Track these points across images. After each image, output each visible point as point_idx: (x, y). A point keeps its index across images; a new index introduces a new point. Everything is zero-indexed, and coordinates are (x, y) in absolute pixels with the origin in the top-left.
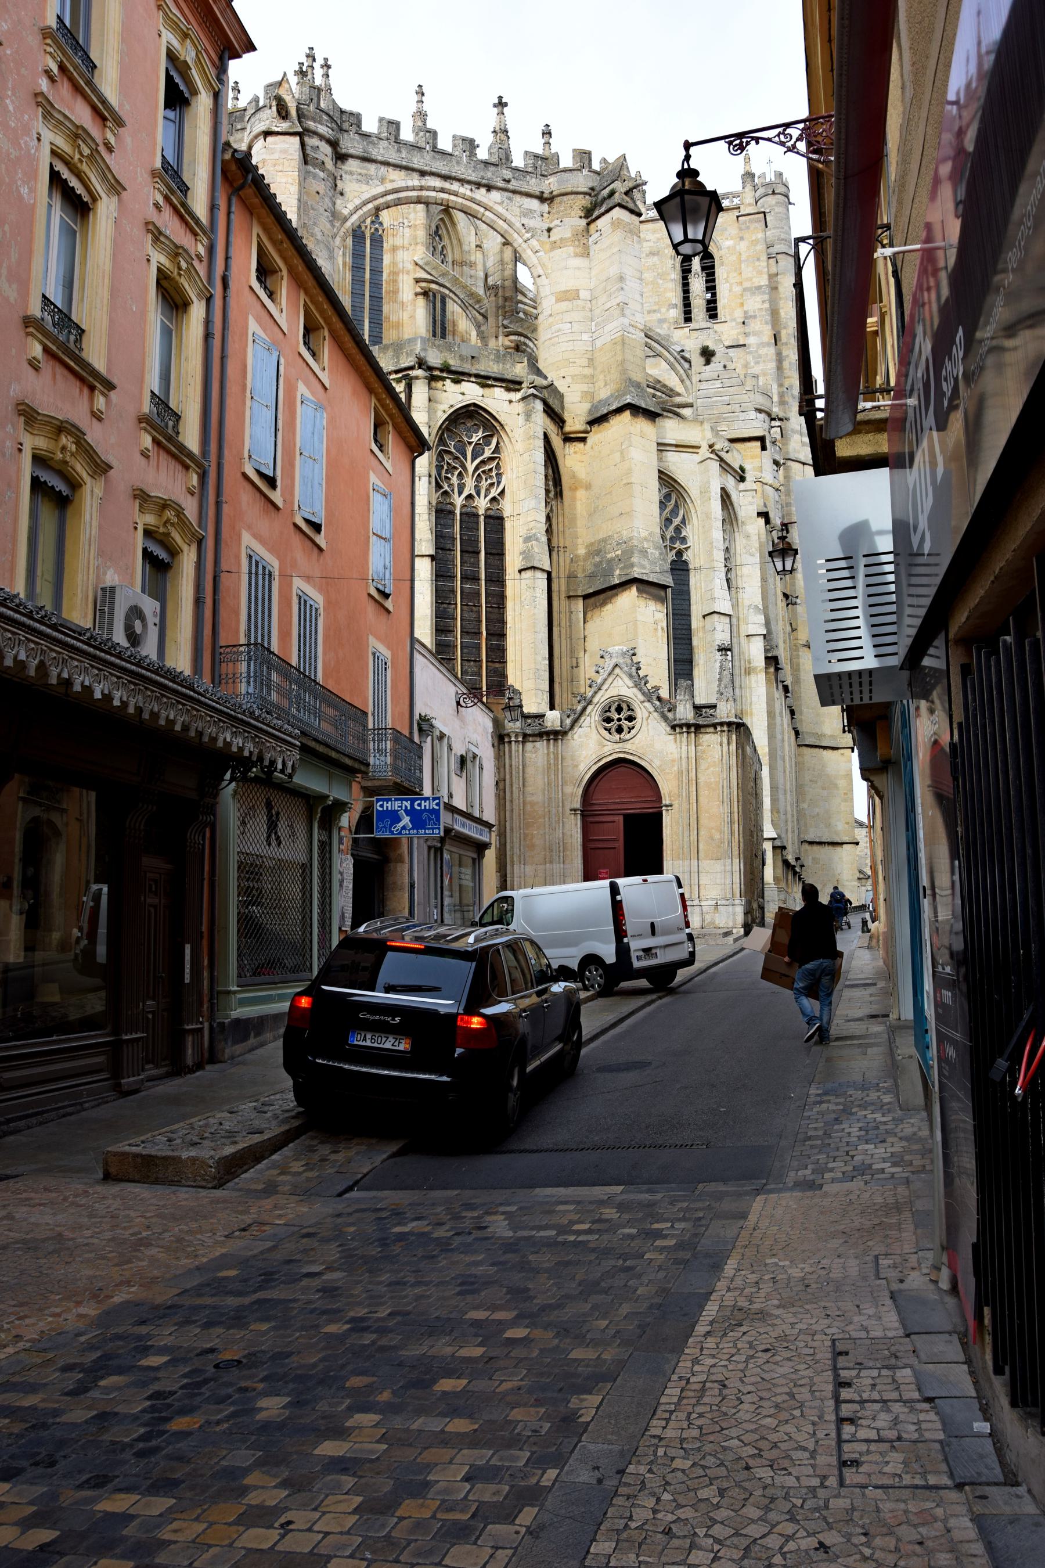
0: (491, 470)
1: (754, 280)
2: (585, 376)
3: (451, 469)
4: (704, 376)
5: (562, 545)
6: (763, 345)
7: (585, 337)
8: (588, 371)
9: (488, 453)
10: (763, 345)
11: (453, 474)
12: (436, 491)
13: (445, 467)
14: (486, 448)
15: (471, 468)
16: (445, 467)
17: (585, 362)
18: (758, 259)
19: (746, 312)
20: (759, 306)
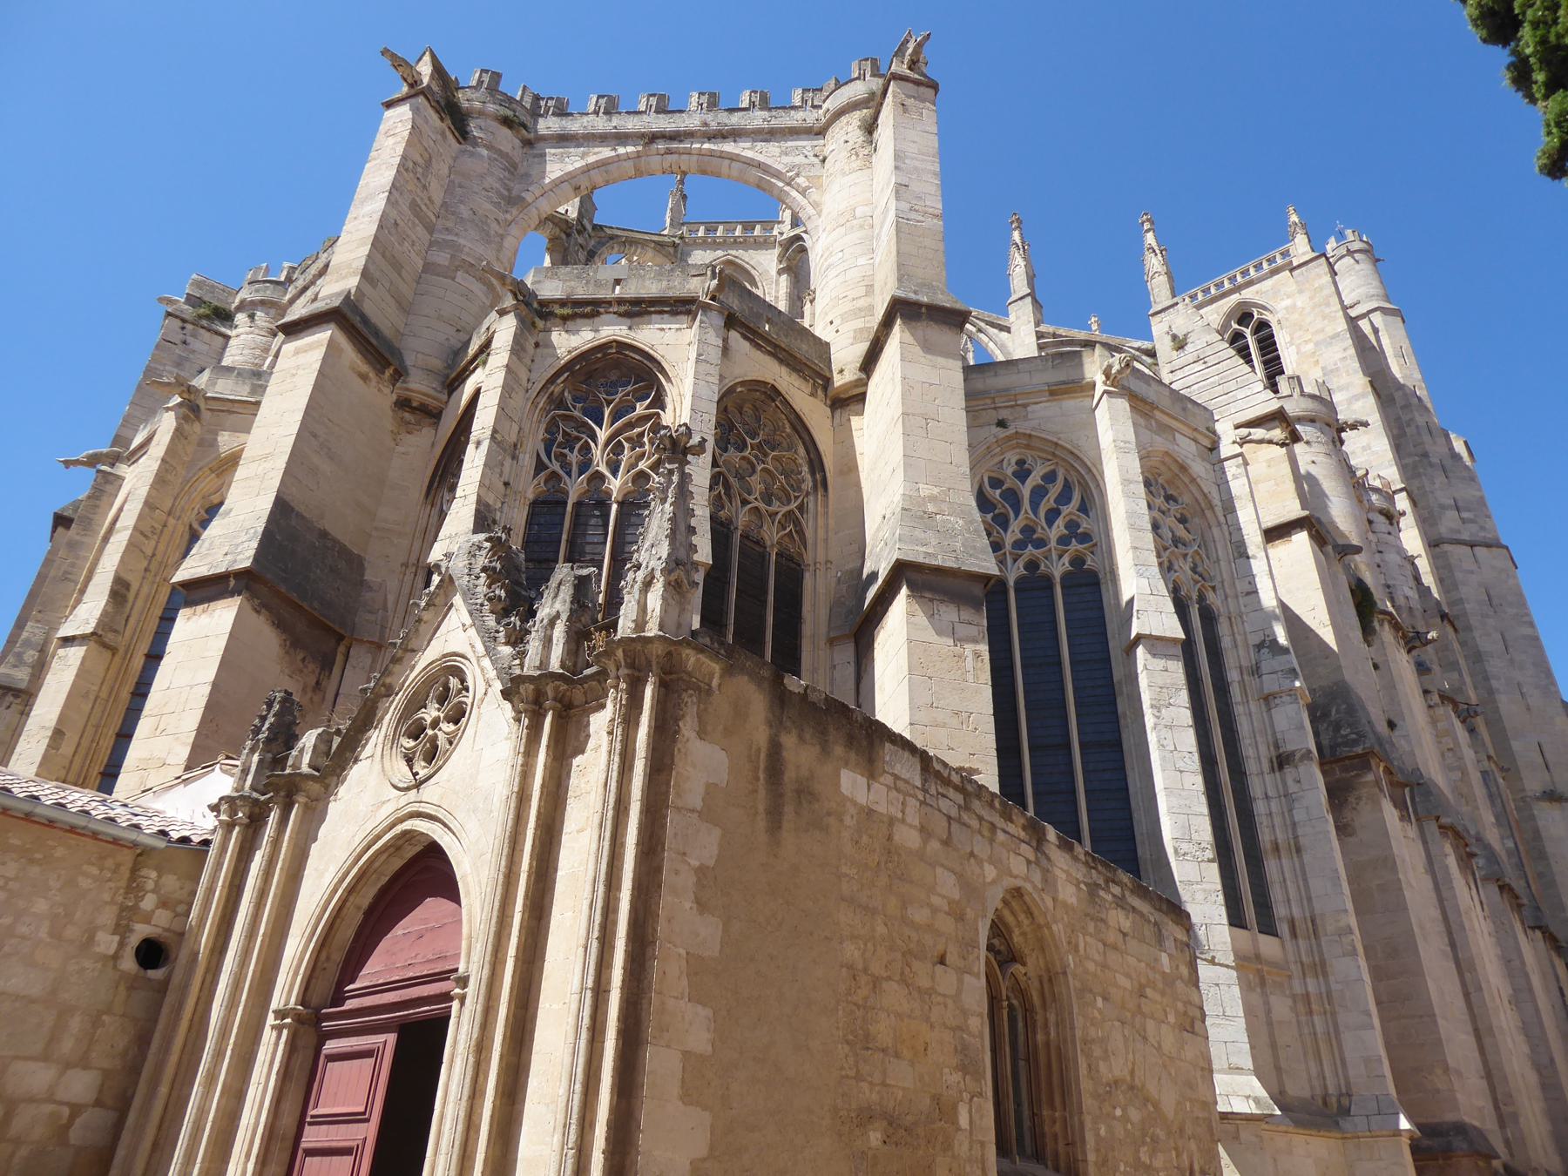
0: (642, 435)
1: (1327, 329)
2: (860, 310)
3: (570, 442)
4: (1177, 364)
5: (821, 558)
6: (1356, 398)
7: (862, 261)
8: (862, 303)
9: (640, 409)
10: (1356, 398)
11: (572, 450)
12: (536, 474)
13: (560, 438)
14: (638, 405)
15: (602, 435)
16: (560, 438)
17: (862, 291)
18: (1328, 305)
19: (1323, 369)
20: (1341, 355)
